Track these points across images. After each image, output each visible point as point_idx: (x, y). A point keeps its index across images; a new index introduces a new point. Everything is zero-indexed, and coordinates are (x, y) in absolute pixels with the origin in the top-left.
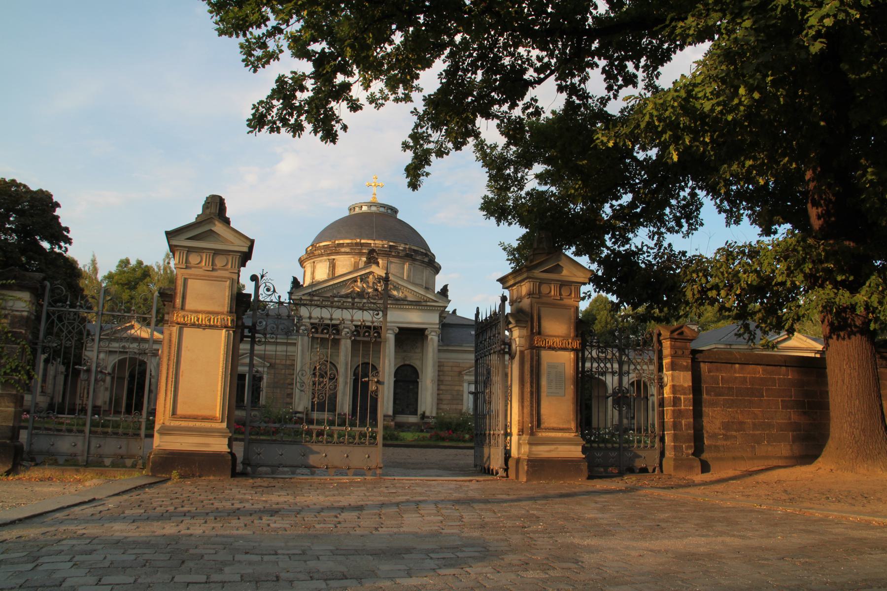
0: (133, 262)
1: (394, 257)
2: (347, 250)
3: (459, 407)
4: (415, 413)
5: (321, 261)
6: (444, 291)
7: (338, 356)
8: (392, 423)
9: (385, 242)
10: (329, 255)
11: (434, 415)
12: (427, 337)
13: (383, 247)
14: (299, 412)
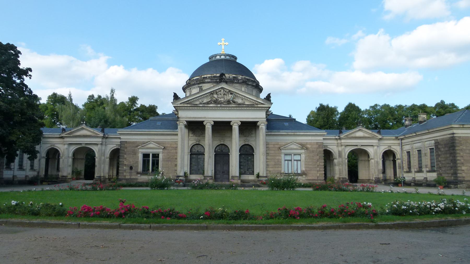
0: (96, 96)
1: (236, 83)
2: (209, 81)
3: (279, 169)
4: (252, 173)
5: (194, 88)
6: (268, 98)
7: (205, 140)
8: (239, 181)
9: (230, 75)
10: (199, 84)
11: (265, 175)
12: (259, 127)
13: (229, 78)
14: (181, 176)
